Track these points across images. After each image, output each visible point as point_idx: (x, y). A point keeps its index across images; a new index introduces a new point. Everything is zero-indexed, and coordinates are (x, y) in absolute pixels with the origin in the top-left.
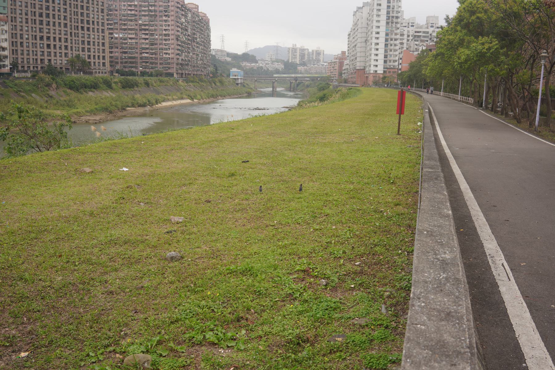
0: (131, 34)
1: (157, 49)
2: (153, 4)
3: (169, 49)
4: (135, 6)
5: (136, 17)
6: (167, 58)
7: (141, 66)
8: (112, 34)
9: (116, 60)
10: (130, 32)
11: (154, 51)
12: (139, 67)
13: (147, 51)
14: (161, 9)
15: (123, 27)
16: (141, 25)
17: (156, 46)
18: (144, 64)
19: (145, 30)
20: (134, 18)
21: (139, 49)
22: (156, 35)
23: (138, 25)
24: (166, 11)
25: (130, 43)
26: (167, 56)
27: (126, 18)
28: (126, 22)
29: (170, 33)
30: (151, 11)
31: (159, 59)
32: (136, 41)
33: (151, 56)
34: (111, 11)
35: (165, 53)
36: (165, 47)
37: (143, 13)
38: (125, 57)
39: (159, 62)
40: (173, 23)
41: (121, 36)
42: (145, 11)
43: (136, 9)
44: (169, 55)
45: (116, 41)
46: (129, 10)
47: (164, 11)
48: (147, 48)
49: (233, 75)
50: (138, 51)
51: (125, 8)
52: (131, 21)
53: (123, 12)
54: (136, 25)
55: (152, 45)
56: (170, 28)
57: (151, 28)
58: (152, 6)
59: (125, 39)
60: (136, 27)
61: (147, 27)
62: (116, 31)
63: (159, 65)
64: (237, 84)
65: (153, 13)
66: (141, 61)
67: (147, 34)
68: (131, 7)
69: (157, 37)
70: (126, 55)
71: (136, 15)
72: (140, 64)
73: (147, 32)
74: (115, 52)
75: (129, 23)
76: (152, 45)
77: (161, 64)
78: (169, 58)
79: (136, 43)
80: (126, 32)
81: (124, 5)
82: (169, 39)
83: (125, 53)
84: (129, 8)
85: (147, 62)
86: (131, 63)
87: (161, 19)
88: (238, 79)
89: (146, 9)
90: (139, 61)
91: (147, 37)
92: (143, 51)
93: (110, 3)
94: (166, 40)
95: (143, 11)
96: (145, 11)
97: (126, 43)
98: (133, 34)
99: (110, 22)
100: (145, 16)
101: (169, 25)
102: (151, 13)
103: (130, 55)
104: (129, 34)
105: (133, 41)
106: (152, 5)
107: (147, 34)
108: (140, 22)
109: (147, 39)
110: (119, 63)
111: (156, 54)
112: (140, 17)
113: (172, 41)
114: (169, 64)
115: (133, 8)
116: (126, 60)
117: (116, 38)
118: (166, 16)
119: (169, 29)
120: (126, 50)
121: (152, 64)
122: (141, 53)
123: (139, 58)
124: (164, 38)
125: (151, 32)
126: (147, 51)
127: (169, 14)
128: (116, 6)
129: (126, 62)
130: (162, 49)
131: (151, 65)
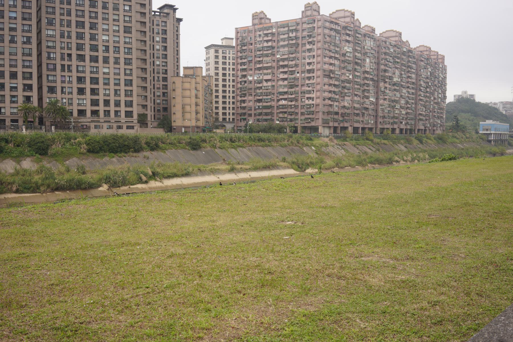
0: (267, 74)
1: (298, 93)
2: (294, 28)
3: (313, 91)
4: (273, 34)
5: (274, 50)
6: (310, 105)
7: (278, 118)
8: (245, 76)
9: (250, 112)
10: (265, 71)
11: (293, 96)
12: (275, 120)
13: (286, 96)
14: (305, 33)
15: (258, 66)
16: (278, 61)
17: (297, 89)
18: (281, 115)
19: (283, 66)
20: (270, 52)
21: (276, 94)
22: (298, 73)
23: (276, 61)
24: (310, 36)
25: (264, 87)
26: (311, 102)
27: (261, 52)
28: (261, 59)
29: (315, 67)
30: (290, 39)
31: (300, 107)
32: (274, 84)
33: (290, 103)
34: (244, 46)
35: (308, 98)
36: (308, 89)
37: (282, 43)
38: (259, 106)
39: (299, 111)
40: (319, 52)
41: (256, 78)
42: (284, 40)
43: (274, 39)
44: (313, 100)
45: (251, 86)
46: (265, 41)
47: (308, 35)
48: (286, 93)
49: (484, 130)
50: (275, 98)
51: (261, 39)
52: (267, 56)
53: (258, 46)
54: (274, 61)
55: (292, 88)
56: (315, 60)
57: (291, 63)
58: (292, 31)
59: (260, 82)
60: (274, 64)
61: (286, 63)
62: (251, 72)
63: (299, 117)
64: (490, 141)
65: (294, 42)
66: (278, 111)
67: (285, 73)
68: (268, 37)
69: (298, 75)
70: (261, 104)
71: (273, 48)
72: (277, 116)
73: (286, 70)
74: (250, 101)
75: (265, 59)
76: (291, 87)
77: (302, 114)
78: (313, 104)
79: (273, 86)
80: (261, 72)
81: (260, 35)
82: (314, 77)
83: (259, 101)
84: (266, 39)
85: (285, 112)
86: (266, 114)
87: (304, 49)
88: (491, 134)
89: (286, 36)
90: (275, 111)
91: (286, 76)
92: (281, 97)
93: (244, 35)
94: (309, 78)
95: (282, 39)
96: (284, 40)
97: (261, 88)
98: (270, 74)
99: (244, 61)
100: (283, 46)
101: (314, 56)
102: (291, 42)
103: (265, 104)
104: (265, 74)
105: (269, 84)
106: (292, 30)
107: (285, 73)
108: (278, 56)
109: (286, 79)
110: (253, 115)
111: (297, 100)
112: (278, 50)
113: (319, 79)
114: (312, 113)
115: (270, 38)
116: (260, 111)
117: (251, 82)
118: (309, 43)
119: (314, 62)
120: (261, 98)
121: (291, 115)
122: (278, 101)
123: (275, 108)
124: (308, 75)
125: (290, 69)
126: (286, 96)
127: (315, 39)
128: (251, 38)
129: (260, 114)
130: (304, 93)
131: (289, 117)
